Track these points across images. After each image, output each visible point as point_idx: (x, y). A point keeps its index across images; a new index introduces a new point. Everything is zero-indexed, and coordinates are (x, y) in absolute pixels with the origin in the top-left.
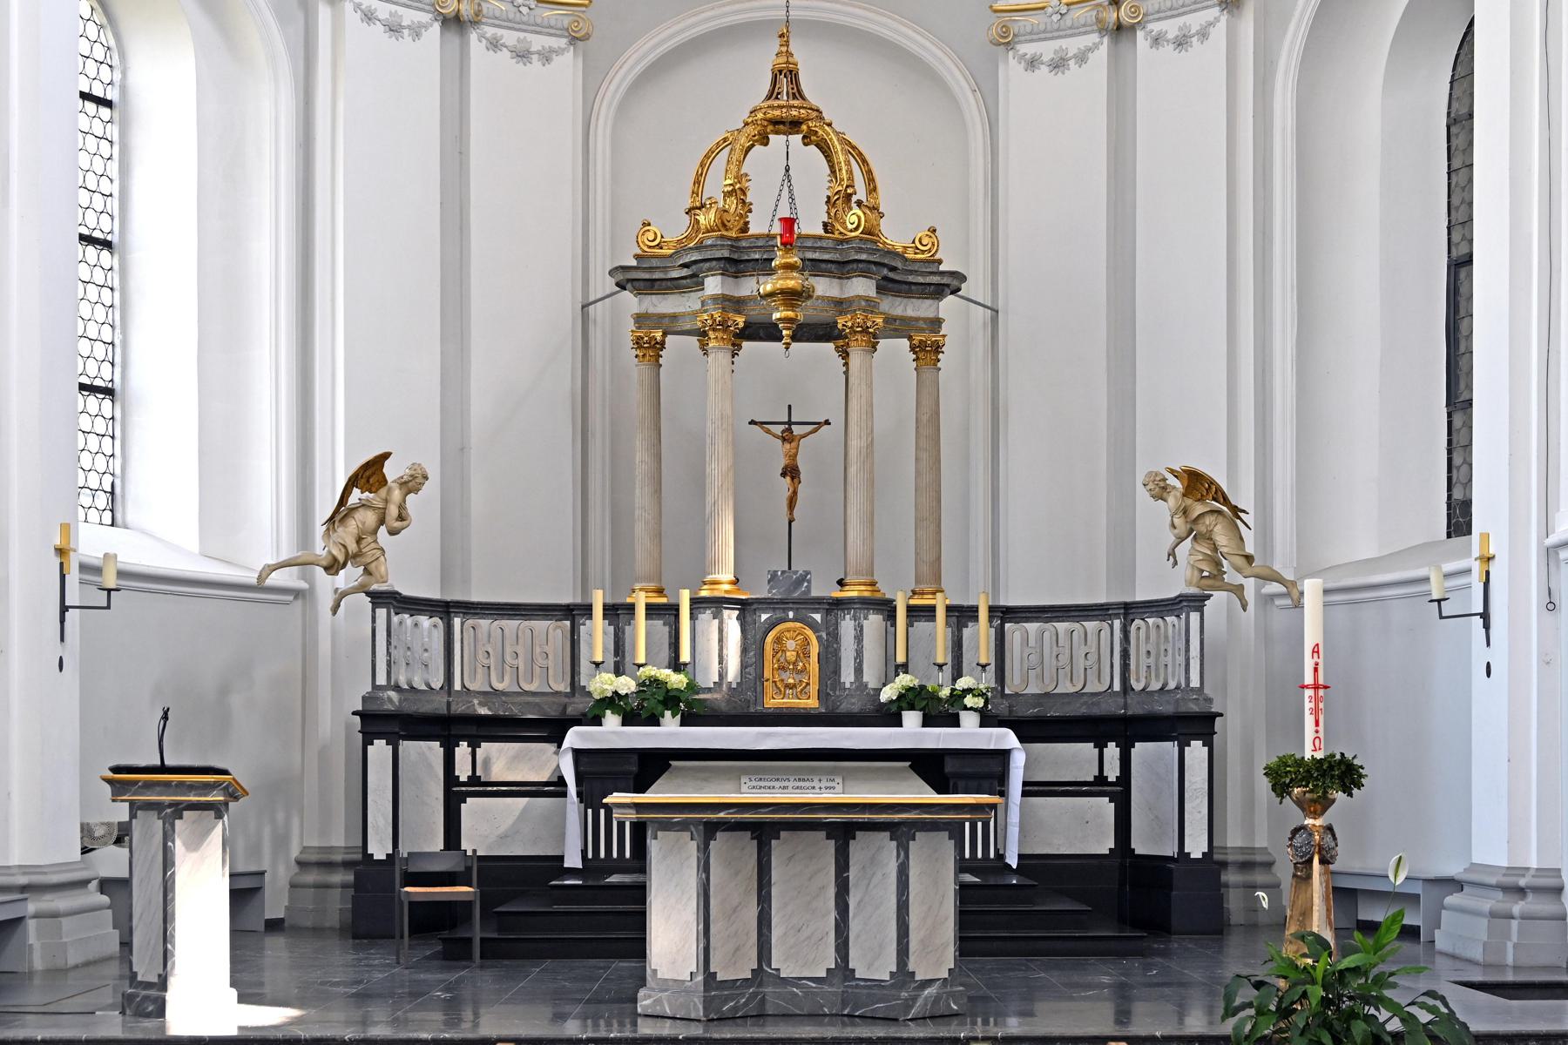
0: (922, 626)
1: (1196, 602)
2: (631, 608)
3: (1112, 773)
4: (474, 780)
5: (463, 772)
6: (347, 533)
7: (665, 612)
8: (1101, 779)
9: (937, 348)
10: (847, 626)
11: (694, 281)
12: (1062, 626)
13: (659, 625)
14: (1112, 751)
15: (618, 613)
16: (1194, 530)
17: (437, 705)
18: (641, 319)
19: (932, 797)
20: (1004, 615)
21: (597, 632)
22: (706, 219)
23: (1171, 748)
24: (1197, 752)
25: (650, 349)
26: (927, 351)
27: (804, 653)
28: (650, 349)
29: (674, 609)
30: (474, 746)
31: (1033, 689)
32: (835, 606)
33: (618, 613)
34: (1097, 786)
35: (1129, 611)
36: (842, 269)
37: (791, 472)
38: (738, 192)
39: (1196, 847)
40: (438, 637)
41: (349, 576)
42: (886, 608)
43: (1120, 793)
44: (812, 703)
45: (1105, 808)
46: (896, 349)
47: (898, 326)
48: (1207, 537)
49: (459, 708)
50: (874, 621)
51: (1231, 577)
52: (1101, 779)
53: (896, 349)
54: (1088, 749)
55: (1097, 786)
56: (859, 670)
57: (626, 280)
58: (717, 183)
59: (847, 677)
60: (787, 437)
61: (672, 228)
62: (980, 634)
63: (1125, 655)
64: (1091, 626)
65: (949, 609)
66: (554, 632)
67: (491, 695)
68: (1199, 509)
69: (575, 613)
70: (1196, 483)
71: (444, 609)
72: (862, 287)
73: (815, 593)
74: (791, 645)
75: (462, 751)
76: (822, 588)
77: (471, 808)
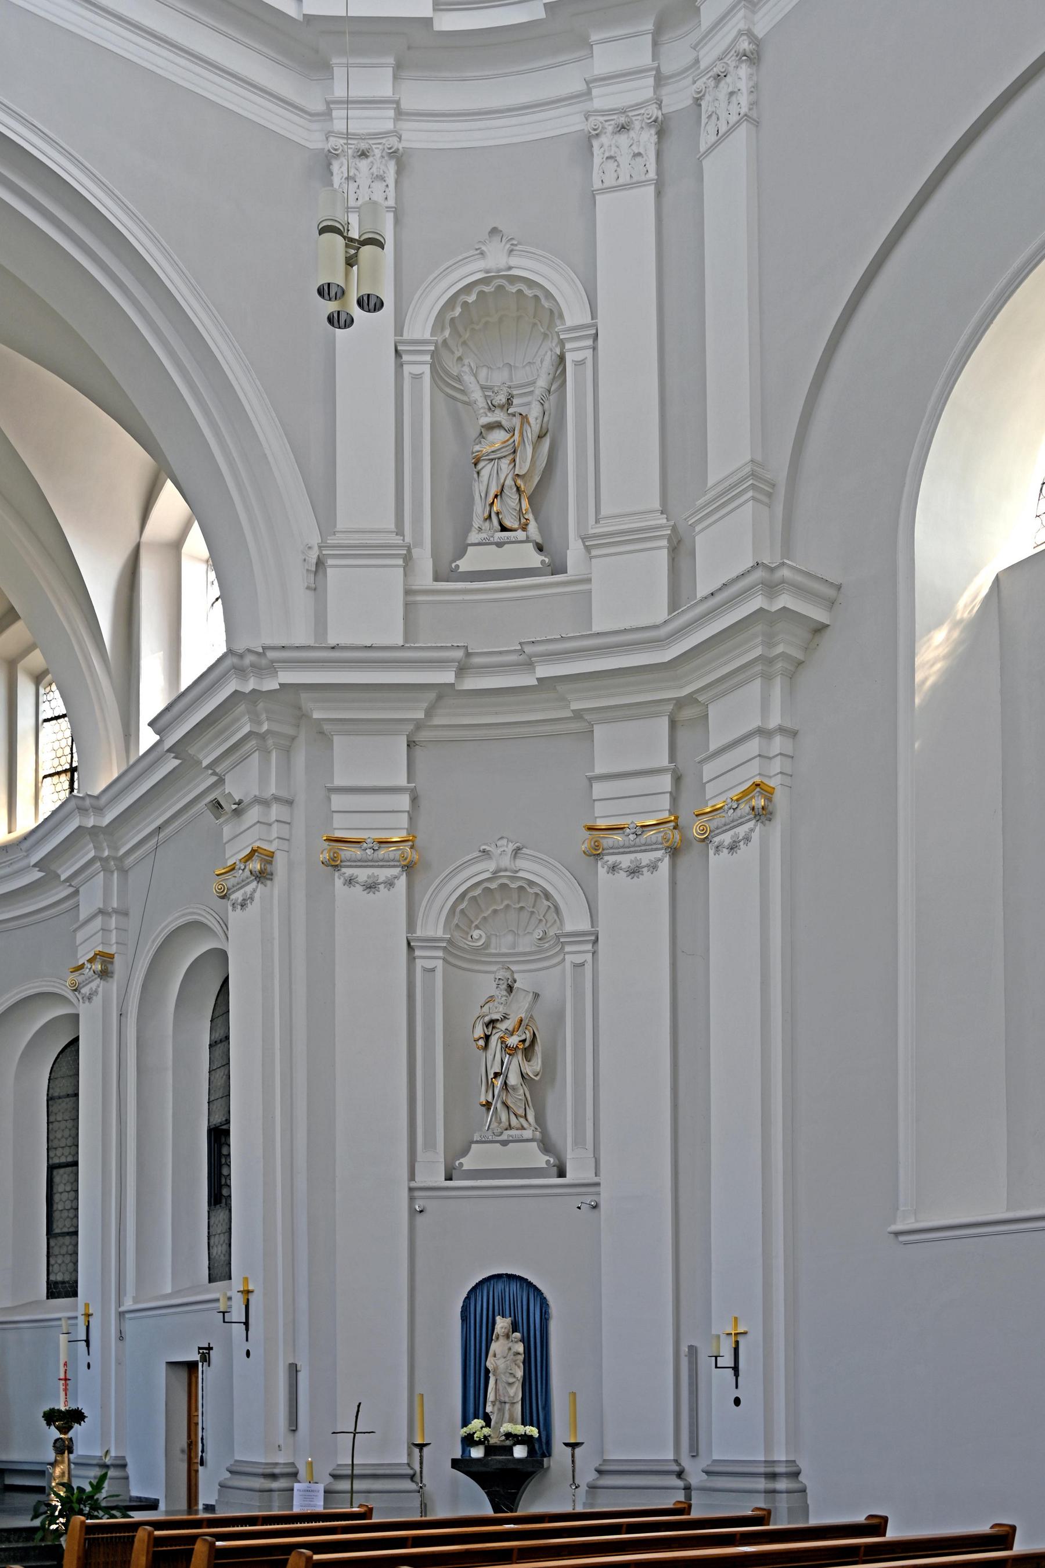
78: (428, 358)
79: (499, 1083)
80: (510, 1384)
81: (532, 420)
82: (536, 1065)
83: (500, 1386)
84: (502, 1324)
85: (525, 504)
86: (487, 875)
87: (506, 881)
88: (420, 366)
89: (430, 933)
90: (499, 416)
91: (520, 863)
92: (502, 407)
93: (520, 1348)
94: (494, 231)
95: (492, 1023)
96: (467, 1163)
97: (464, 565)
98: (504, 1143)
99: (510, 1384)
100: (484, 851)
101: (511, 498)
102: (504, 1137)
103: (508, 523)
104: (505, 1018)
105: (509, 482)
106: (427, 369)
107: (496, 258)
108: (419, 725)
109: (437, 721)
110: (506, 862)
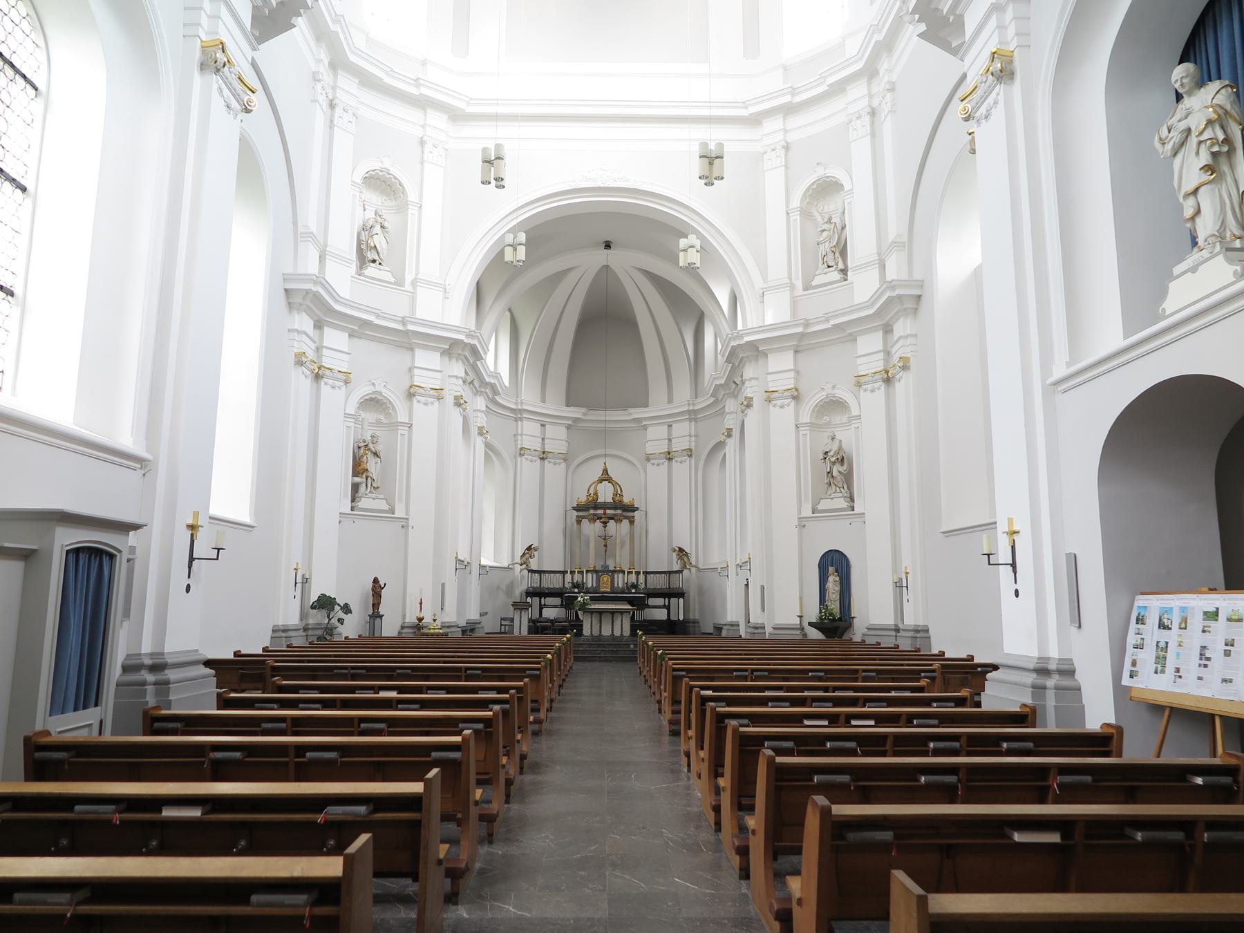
0: (630, 575)
1: (681, 572)
2: (575, 572)
3: (667, 604)
4: (545, 605)
5: (543, 603)
6: (524, 559)
7: (581, 572)
8: (665, 605)
9: (634, 521)
10: (616, 576)
11: (587, 509)
12: (658, 575)
13: (580, 575)
14: (667, 600)
15: (572, 573)
16: (680, 558)
17: (538, 591)
18: (577, 516)
19: (631, 608)
20: (646, 573)
21: (568, 576)
22: (590, 499)
23: (677, 599)
24: (681, 600)
25: (579, 522)
26: (632, 522)
27: (608, 581)
28: (579, 522)
29: (583, 572)
30: (545, 598)
31: (652, 587)
32: (614, 572)
33: (572, 573)
34: (664, 606)
35: (670, 573)
36: (615, 508)
37: (606, 546)
38: (596, 494)
39: (681, 618)
40: (539, 577)
41: (524, 566)
42: (624, 572)
43: (668, 608)
44: (609, 590)
45: (665, 611)
46: (626, 522)
47: (626, 517)
48: (682, 559)
49: (542, 591)
50: (621, 575)
51: (688, 567)
52: (665, 605)
53: (626, 522)
54: (662, 599)
55: (664, 606)
56: (618, 584)
57: (574, 508)
58: (592, 492)
59: (616, 585)
60: (605, 539)
61: (583, 499)
62: (642, 577)
63: (669, 581)
64: (663, 575)
65: (635, 572)
66: (560, 576)
67: (548, 588)
68: (681, 554)
69: (564, 573)
70: (681, 550)
71: (540, 572)
72: (619, 512)
73: (610, 569)
74: (605, 579)
75: (543, 599)
76: (611, 568)
77: (544, 610)
78: (798, 213)
79: (830, 475)
80: (833, 593)
81: (837, 225)
82: (845, 467)
83: (830, 593)
84: (831, 569)
85: (837, 255)
86: (825, 397)
87: (831, 398)
88: (796, 216)
89: (805, 421)
90: (826, 226)
91: (836, 391)
92: (827, 223)
93: (837, 579)
94: (818, 164)
95: (827, 452)
96: (820, 507)
97: (814, 283)
98: (832, 499)
99: (833, 593)
100: (823, 388)
101: (831, 256)
102: (832, 497)
103: (830, 264)
104: (830, 451)
105: (829, 250)
106: (798, 217)
107: (820, 172)
108: (797, 346)
109: (803, 343)
110: (830, 391)
